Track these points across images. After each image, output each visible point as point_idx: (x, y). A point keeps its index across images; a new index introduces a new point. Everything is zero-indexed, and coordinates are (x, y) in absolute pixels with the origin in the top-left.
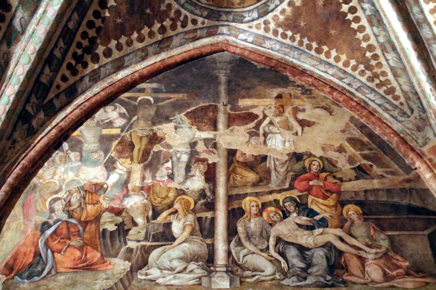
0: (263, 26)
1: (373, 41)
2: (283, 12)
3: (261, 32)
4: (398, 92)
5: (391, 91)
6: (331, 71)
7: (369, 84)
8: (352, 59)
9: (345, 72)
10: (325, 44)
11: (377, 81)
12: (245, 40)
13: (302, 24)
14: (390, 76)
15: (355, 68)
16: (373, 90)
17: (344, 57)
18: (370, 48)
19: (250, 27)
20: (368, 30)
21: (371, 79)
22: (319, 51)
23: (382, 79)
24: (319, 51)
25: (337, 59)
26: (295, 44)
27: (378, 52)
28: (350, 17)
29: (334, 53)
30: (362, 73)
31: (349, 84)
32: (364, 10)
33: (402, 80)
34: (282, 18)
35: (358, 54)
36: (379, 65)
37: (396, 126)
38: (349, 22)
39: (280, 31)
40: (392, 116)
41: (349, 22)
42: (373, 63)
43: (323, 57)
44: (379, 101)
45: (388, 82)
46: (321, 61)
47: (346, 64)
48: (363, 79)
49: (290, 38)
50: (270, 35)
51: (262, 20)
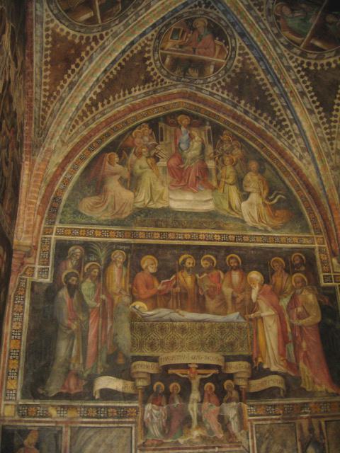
0: (49, 19)
1: (62, 91)
2: (62, 30)
3: (45, 19)
4: (45, 122)
5: (44, 118)
6: (38, 77)
7: (41, 104)
8: (50, 86)
9: (41, 86)
10: (51, 65)
11: (44, 107)
12: (36, 10)
13: (58, 46)
14: (49, 112)
15: (45, 90)
16: (39, 108)
17: (48, 80)
18: (58, 92)
19: (46, 10)
20: (66, 85)
21: (45, 104)
22: (46, 63)
23: (47, 109)
24: (46, 63)
25: (46, 77)
26: (45, 45)
27: (58, 97)
28: (69, 72)
29: (48, 73)
30: (45, 96)
31: (36, 93)
32: (74, 77)
33: (51, 119)
34: (58, 30)
35: (53, 87)
36: (52, 102)
37: (32, 136)
38: (67, 73)
39: (50, 32)
40: (35, 129)
41: (67, 73)
42: (52, 99)
43: (44, 67)
44: (37, 117)
45: (46, 113)
46: (40, 68)
47: (45, 84)
48: (42, 99)
49: (48, 41)
50: (45, 26)
51: (53, 17)
